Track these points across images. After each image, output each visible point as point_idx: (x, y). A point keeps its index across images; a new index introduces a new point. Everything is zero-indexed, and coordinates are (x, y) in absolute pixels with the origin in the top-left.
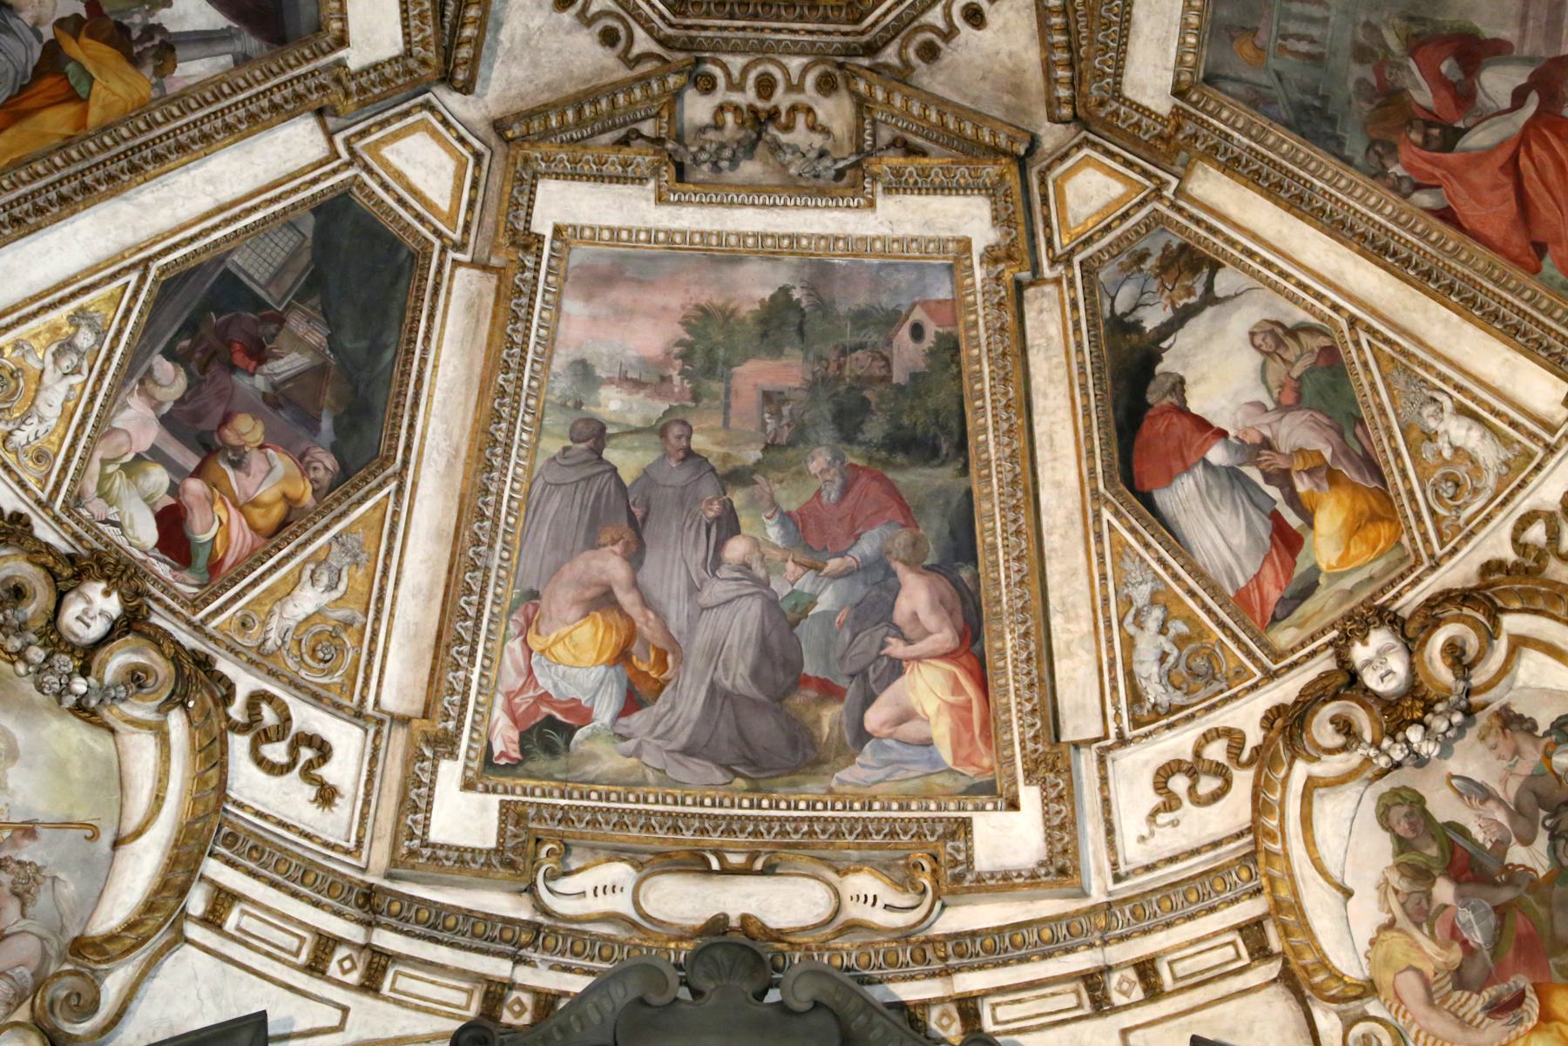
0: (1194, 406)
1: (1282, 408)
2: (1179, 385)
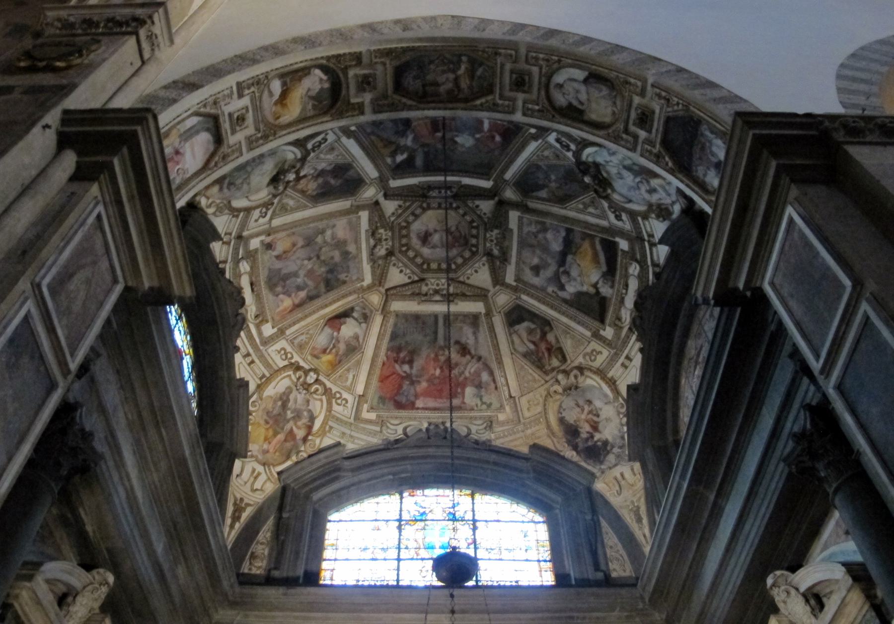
0: (342, 327)
1: (345, 342)
2: (345, 323)
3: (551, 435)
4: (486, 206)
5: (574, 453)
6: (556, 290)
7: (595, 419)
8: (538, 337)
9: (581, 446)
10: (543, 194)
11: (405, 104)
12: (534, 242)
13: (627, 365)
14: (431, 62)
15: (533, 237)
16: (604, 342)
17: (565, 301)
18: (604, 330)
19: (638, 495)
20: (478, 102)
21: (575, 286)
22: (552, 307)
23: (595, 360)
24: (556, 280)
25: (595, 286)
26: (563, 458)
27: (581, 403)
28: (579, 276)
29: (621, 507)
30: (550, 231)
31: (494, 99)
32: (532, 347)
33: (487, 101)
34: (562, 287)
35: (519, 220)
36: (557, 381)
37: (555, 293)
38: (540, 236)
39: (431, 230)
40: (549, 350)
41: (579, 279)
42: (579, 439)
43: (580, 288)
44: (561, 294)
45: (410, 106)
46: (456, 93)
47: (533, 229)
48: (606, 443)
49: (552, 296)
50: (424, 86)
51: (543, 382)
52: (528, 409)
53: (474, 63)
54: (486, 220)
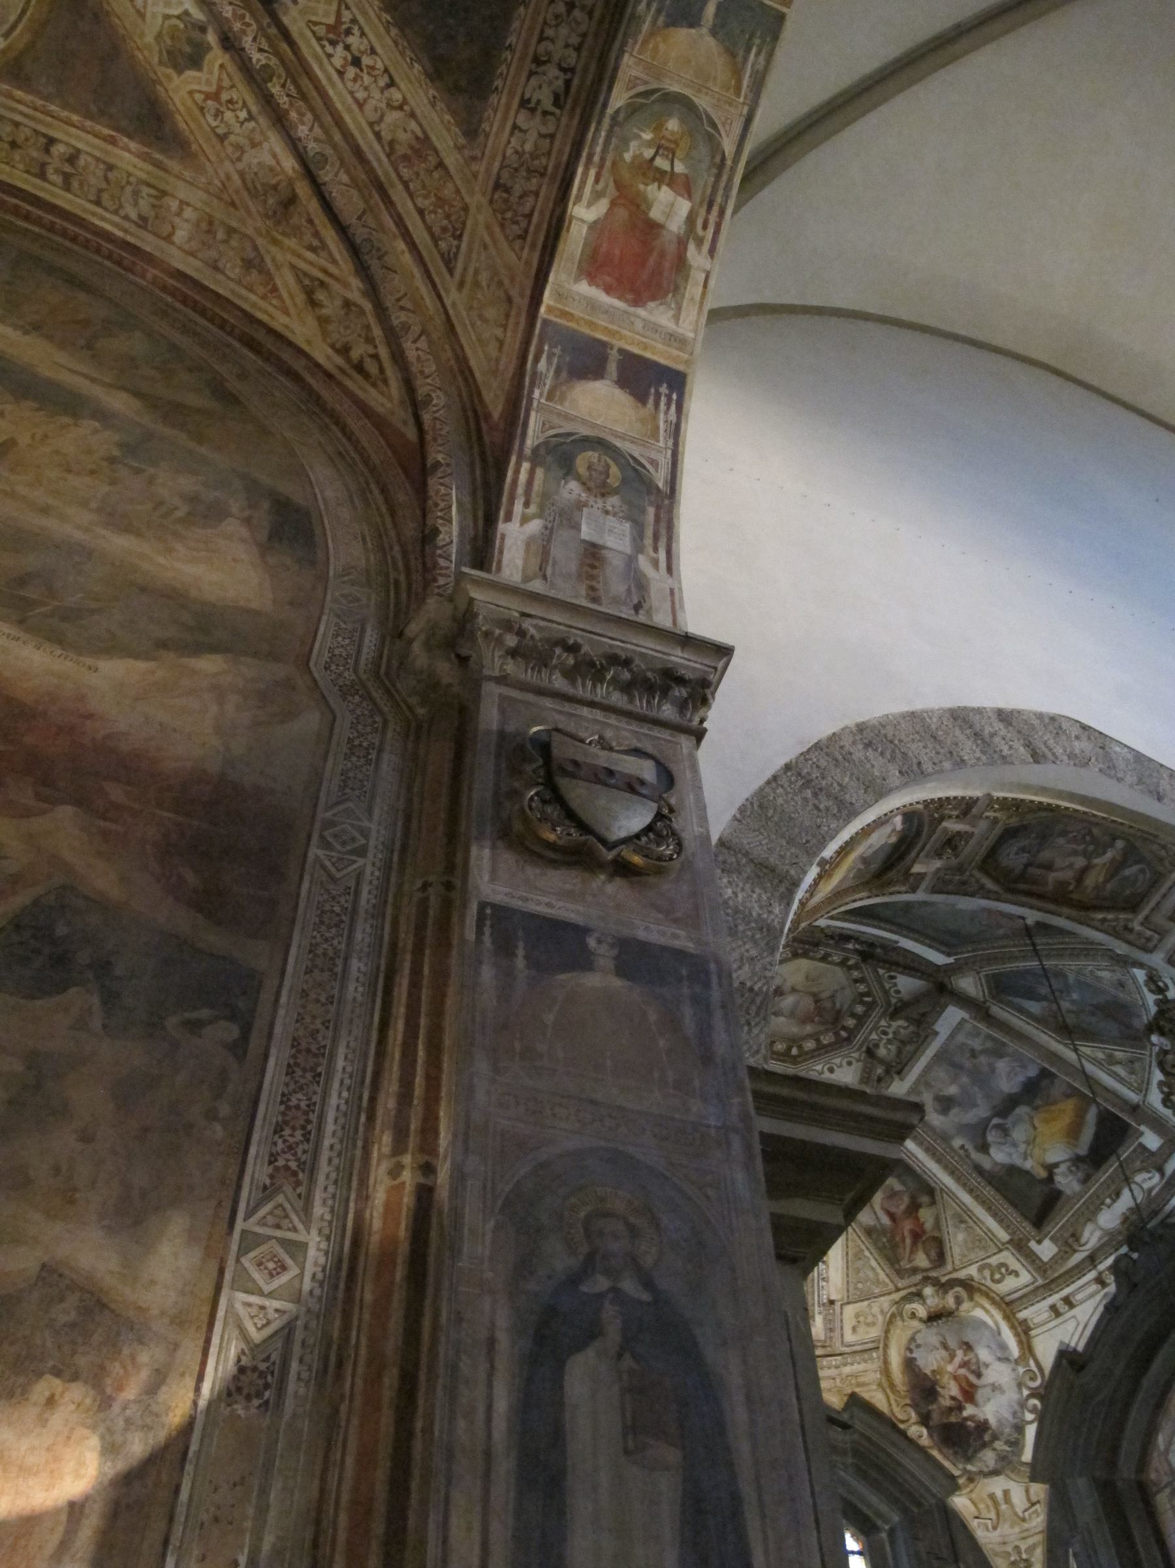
3: (886, 1384)
4: (907, 984)
5: (925, 1431)
6: (969, 1146)
7: (972, 1378)
8: (903, 1207)
9: (936, 1418)
10: (1034, 1007)
11: (982, 887)
12: (968, 1064)
13: (1061, 1310)
14: (1064, 833)
15: (968, 1055)
16: (1033, 1262)
17: (979, 1169)
18: (1039, 1242)
19: (1031, 1541)
20: (1100, 916)
21: (1010, 1155)
22: (952, 1172)
23: (999, 1281)
24: (980, 1137)
25: (1051, 1168)
26: (903, 1434)
27: (952, 1343)
28: (1027, 1143)
29: (996, 1554)
30: (1006, 1059)
31: (1132, 921)
32: (886, 1220)
33: (1116, 919)
34: (984, 1148)
35: (960, 1023)
36: (919, 1295)
37: (966, 1151)
38: (983, 1059)
39: (787, 987)
40: (917, 1236)
41: (1022, 1147)
42: (934, 1407)
43: (1017, 1161)
44: (976, 1156)
45: (989, 891)
46: (1071, 888)
47: (977, 1044)
48: (983, 1426)
49: (960, 1156)
50: (1026, 866)
51: (891, 1287)
52: (854, 1329)
53: (1131, 854)
54: (893, 1001)
